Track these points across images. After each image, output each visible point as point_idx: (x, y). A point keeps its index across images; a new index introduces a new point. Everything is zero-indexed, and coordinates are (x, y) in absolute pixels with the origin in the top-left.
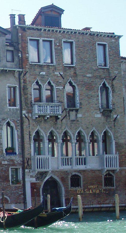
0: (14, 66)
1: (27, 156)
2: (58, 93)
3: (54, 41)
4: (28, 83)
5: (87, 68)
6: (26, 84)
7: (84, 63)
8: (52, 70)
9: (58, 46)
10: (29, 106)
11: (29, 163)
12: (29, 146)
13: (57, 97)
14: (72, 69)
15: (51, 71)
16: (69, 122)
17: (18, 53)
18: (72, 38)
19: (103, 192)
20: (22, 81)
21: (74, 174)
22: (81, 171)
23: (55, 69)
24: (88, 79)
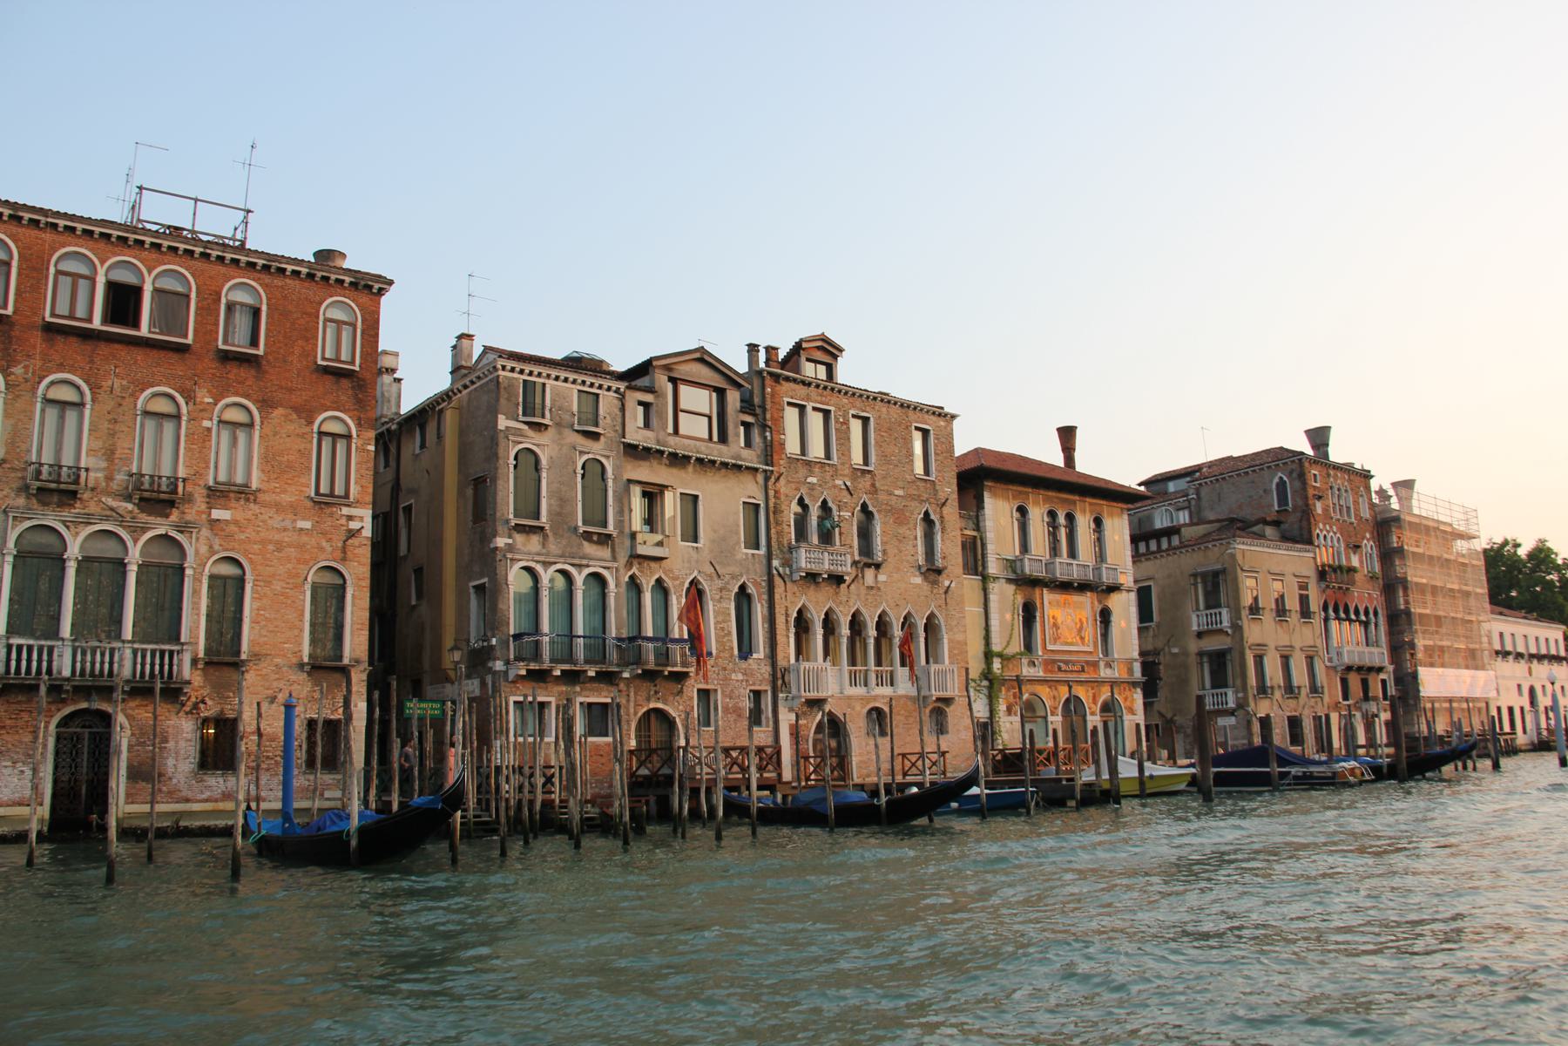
0: (755, 459)
1: (781, 663)
4: (783, 497)
6: (778, 502)
10: (785, 550)
11: (786, 679)
14: (868, 476)
16: (863, 591)
17: (765, 431)
20: (771, 493)
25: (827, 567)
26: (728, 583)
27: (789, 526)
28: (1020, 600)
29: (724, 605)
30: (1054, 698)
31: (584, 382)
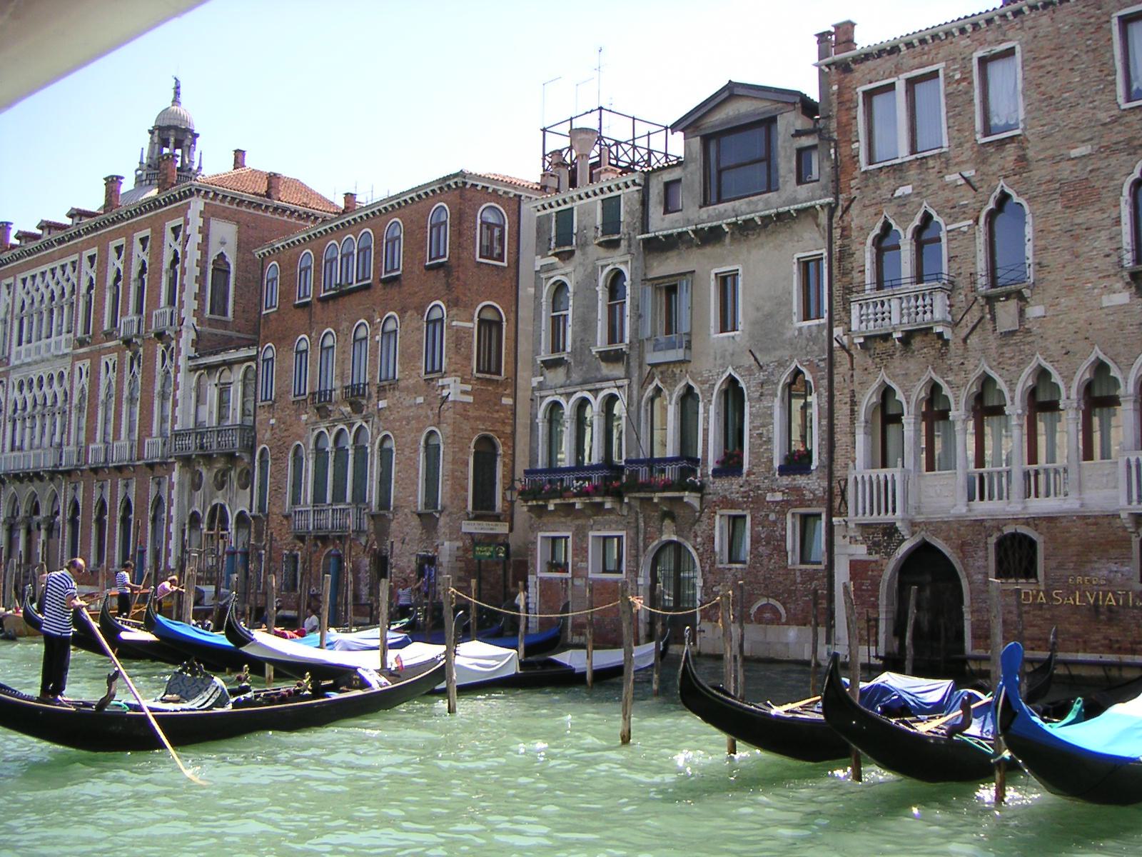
0: (818, 193)
1: (838, 473)
2: (954, 244)
3: (945, 69)
4: (854, 234)
5: (1072, 125)
7: (1057, 110)
8: (936, 169)
9: (958, 82)
12: (847, 439)
14: (1011, 151)
15: (932, 175)
16: (993, 343)
18: (1010, 34)
19: (1131, 604)
20: (837, 233)
21: (1008, 530)
22: (1039, 518)
23: (944, 165)
24: (1074, 165)
27: (863, 271)
29: (766, 404)
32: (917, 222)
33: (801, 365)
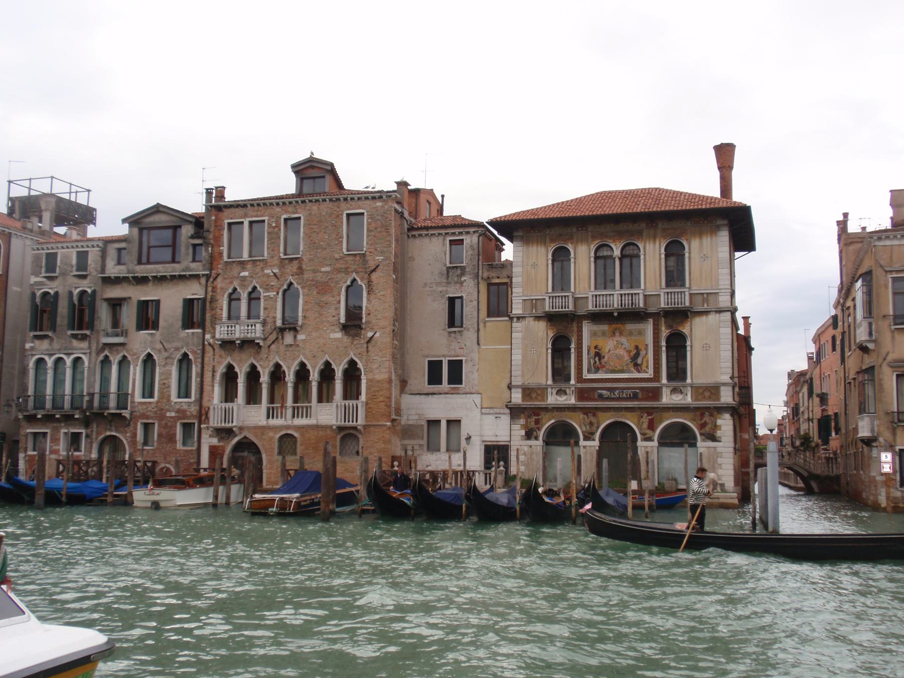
0: (201, 268)
1: (205, 403)
2: (267, 302)
4: (218, 291)
8: (261, 266)
9: (274, 228)
13: (265, 309)
14: (295, 264)
15: (258, 269)
16: (282, 348)
18: (299, 210)
20: (210, 289)
25: (237, 335)
26: (172, 354)
27: (222, 309)
28: (551, 334)
30: (591, 424)
31: (77, 246)
32: (250, 289)
33: (188, 350)
